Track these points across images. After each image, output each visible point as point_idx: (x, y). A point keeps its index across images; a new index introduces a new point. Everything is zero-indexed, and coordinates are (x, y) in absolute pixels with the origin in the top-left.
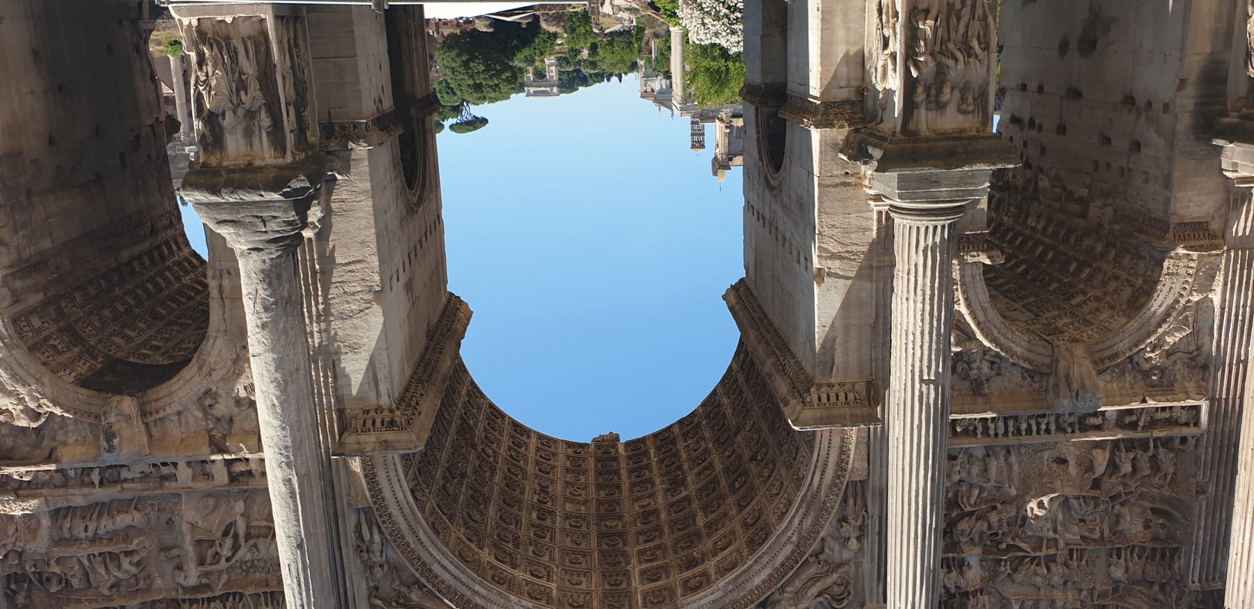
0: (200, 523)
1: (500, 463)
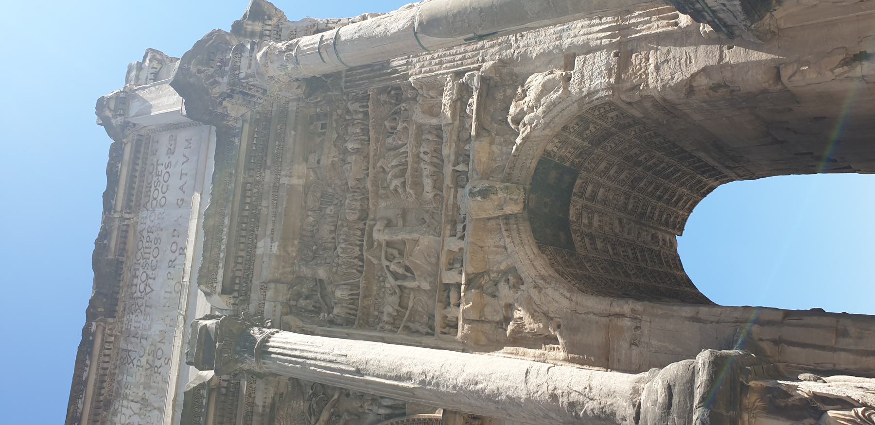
0: (418, 248)
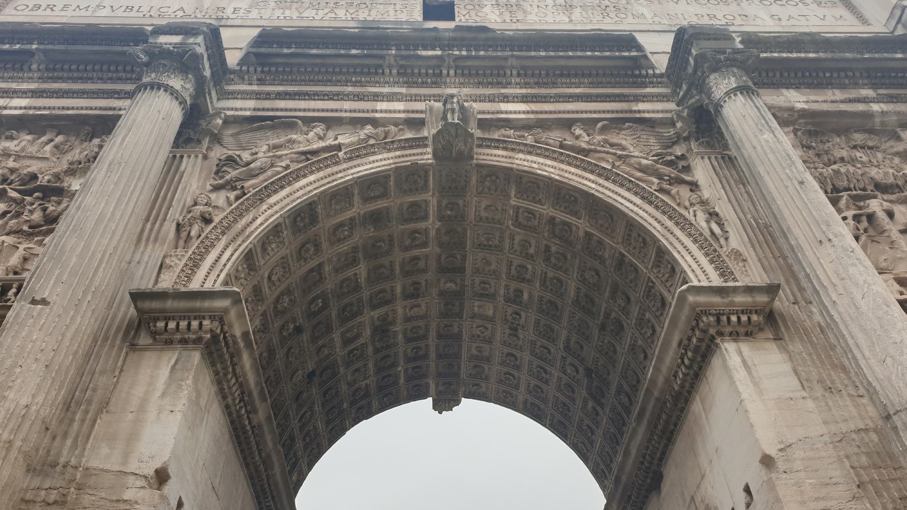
1: (559, 357)
